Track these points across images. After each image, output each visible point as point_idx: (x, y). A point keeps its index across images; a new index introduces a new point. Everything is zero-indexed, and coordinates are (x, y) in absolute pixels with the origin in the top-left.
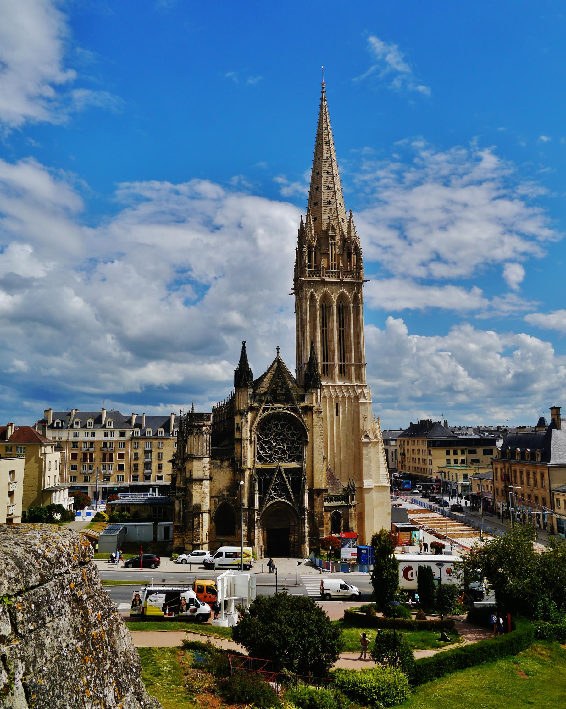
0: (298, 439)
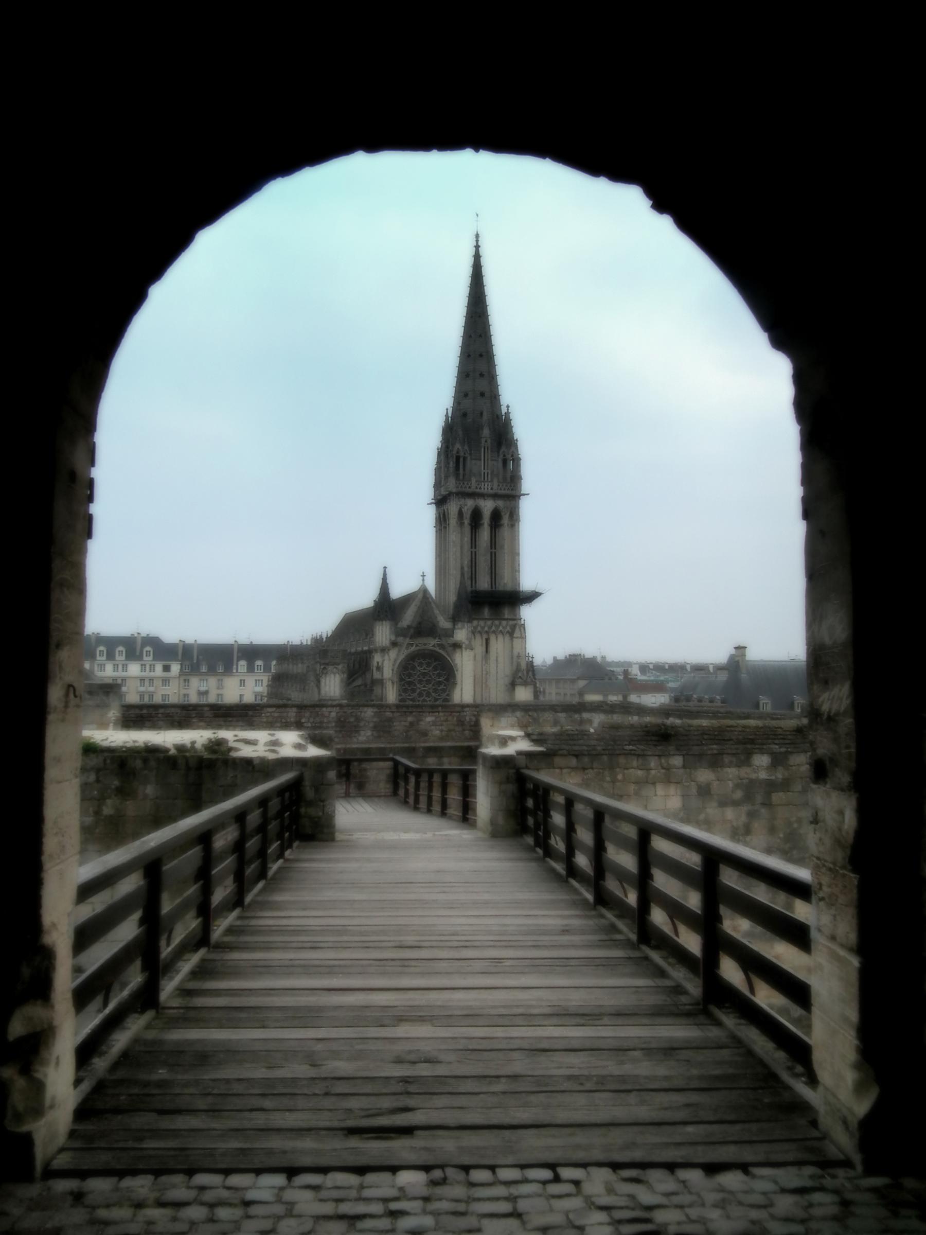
0: (445, 680)
